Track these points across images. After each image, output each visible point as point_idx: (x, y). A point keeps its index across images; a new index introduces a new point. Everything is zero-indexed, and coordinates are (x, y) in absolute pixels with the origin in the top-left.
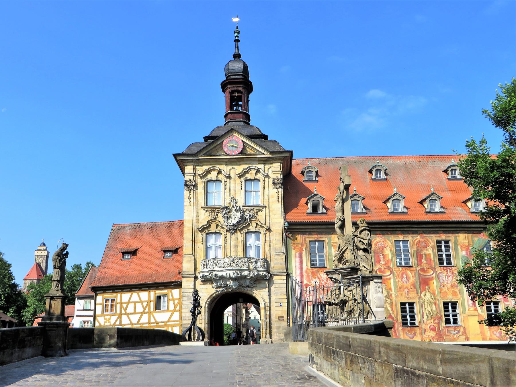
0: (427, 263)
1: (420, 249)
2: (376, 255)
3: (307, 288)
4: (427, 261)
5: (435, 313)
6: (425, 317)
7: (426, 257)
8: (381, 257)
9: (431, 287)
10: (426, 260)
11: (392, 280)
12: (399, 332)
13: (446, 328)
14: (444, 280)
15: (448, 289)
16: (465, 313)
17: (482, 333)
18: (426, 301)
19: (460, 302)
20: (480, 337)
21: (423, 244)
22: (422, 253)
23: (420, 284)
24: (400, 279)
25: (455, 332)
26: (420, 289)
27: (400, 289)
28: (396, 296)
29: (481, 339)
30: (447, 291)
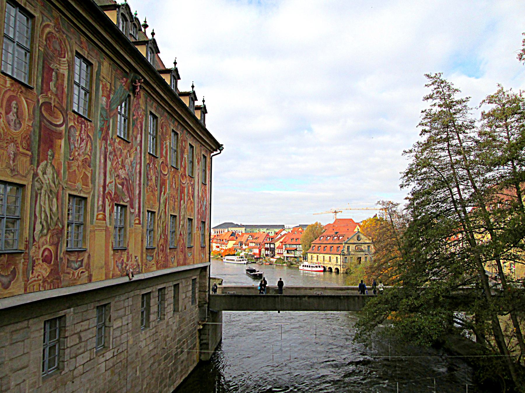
0: (56, 95)
4: (57, 89)
5: (55, 219)
6: (38, 227)
7: (57, 80)
9: (56, 156)
13: (67, 256)
14: (76, 145)
15: (78, 167)
16: (92, 224)
17: (107, 264)
18: (45, 186)
19: (89, 201)
20: (104, 271)
23: (39, 141)
25: (76, 266)
26: (38, 155)
29: (104, 278)
30: (77, 171)
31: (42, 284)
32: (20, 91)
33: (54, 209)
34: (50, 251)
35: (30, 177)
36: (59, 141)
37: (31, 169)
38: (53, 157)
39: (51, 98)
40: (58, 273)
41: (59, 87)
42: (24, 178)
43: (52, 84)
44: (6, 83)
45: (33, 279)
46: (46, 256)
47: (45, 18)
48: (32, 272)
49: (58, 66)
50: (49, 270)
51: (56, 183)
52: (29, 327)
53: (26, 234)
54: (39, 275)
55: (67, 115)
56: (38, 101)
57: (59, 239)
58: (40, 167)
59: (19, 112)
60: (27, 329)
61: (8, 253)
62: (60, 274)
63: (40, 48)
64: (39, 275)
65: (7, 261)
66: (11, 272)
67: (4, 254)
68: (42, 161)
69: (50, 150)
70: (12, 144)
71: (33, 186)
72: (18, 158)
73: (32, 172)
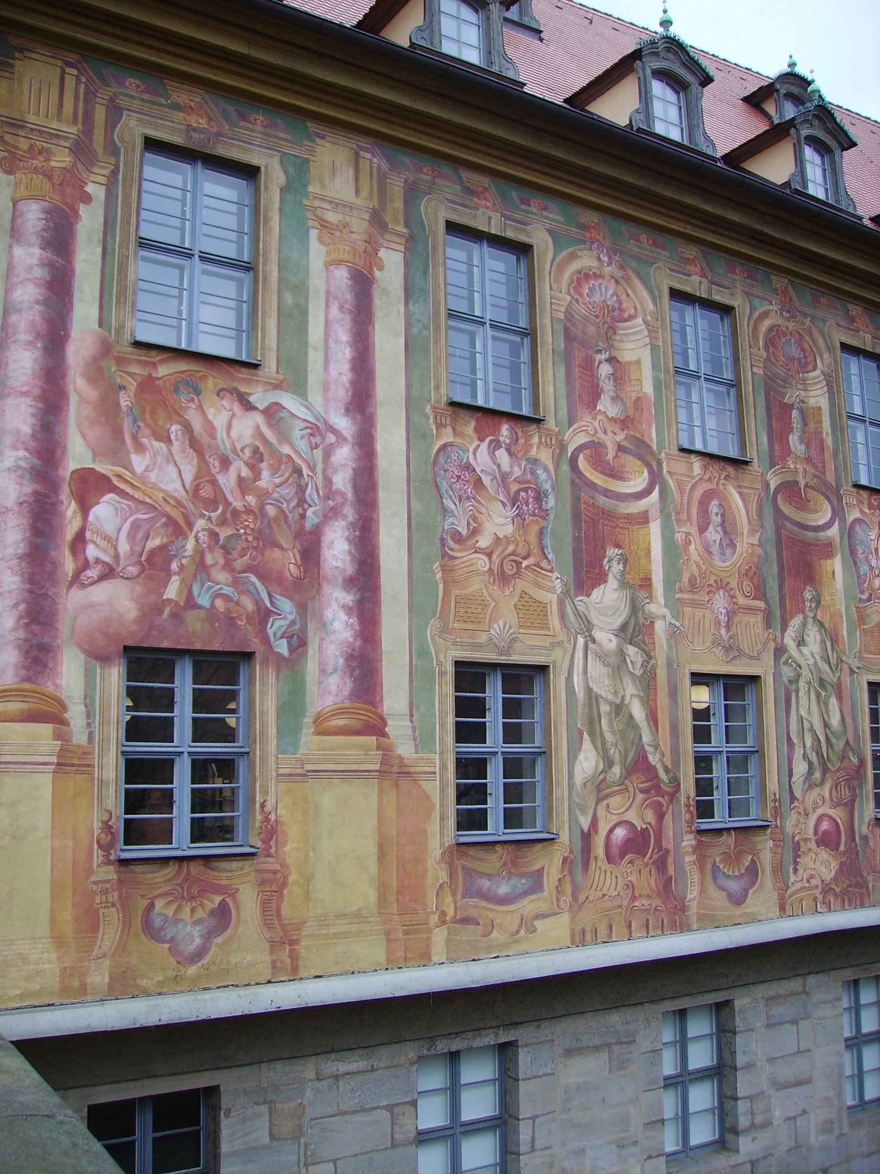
0: (808, 460)
1: (781, 372)
2: (578, 355)
3: (85, 508)
4: (808, 446)
5: (839, 745)
6: (800, 768)
7: (805, 424)
8: (605, 370)
9: (826, 598)
10: (805, 440)
11: (655, 529)
12: (679, 867)
18: (805, 672)
21: (794, 352)
22: (791, 396)
23: (781, 572)
24: (694, 530)
26: (782, 604)
27: (690, 588)
28: (674, 633)
31: (820, 897)
32: (722, 477)
33: (835, 721)
34: (835, 821)
35: (769, 658)
36: (829, 562)
37: (768, 638)
38: (818, 603)
39: (796, 471)
40: (858, 873)
41: (813, 440)
42: (754, 662)
43: (794, 440)
44: (692, 468)
45: (798, 886)
46: (826, 832)
47: (756, 301)
48: (796, 870)
49: (803, 394)
50: (834, 865)
51: (833, 661)
52: (807, 993)
53: (773, 783)
54: (812, 877)
55: (840, 498)
56: (768, 485)
57: (854, 789)
58: (790, 633)
59: (727, 525)
60: (804, 997)
61: (735, 829)
62: (865, 873)
63: (755, 370)
64: (812, 877)
65: (736, 846)
66: (747, 869)
67: (728, 830)
68: (792, 617)
69: (808, 588)
70: (721, 592)
71: (777, 676)
72: (736, 619)
73: (772, 645)
